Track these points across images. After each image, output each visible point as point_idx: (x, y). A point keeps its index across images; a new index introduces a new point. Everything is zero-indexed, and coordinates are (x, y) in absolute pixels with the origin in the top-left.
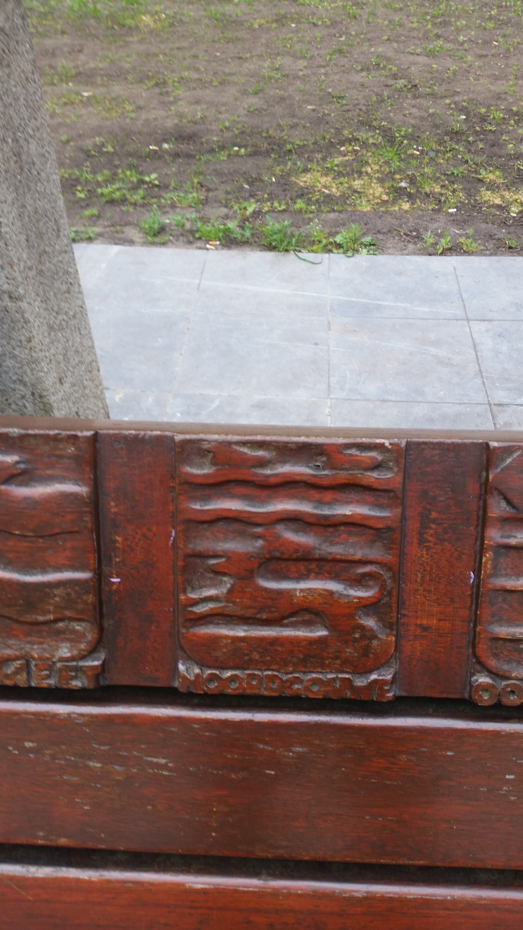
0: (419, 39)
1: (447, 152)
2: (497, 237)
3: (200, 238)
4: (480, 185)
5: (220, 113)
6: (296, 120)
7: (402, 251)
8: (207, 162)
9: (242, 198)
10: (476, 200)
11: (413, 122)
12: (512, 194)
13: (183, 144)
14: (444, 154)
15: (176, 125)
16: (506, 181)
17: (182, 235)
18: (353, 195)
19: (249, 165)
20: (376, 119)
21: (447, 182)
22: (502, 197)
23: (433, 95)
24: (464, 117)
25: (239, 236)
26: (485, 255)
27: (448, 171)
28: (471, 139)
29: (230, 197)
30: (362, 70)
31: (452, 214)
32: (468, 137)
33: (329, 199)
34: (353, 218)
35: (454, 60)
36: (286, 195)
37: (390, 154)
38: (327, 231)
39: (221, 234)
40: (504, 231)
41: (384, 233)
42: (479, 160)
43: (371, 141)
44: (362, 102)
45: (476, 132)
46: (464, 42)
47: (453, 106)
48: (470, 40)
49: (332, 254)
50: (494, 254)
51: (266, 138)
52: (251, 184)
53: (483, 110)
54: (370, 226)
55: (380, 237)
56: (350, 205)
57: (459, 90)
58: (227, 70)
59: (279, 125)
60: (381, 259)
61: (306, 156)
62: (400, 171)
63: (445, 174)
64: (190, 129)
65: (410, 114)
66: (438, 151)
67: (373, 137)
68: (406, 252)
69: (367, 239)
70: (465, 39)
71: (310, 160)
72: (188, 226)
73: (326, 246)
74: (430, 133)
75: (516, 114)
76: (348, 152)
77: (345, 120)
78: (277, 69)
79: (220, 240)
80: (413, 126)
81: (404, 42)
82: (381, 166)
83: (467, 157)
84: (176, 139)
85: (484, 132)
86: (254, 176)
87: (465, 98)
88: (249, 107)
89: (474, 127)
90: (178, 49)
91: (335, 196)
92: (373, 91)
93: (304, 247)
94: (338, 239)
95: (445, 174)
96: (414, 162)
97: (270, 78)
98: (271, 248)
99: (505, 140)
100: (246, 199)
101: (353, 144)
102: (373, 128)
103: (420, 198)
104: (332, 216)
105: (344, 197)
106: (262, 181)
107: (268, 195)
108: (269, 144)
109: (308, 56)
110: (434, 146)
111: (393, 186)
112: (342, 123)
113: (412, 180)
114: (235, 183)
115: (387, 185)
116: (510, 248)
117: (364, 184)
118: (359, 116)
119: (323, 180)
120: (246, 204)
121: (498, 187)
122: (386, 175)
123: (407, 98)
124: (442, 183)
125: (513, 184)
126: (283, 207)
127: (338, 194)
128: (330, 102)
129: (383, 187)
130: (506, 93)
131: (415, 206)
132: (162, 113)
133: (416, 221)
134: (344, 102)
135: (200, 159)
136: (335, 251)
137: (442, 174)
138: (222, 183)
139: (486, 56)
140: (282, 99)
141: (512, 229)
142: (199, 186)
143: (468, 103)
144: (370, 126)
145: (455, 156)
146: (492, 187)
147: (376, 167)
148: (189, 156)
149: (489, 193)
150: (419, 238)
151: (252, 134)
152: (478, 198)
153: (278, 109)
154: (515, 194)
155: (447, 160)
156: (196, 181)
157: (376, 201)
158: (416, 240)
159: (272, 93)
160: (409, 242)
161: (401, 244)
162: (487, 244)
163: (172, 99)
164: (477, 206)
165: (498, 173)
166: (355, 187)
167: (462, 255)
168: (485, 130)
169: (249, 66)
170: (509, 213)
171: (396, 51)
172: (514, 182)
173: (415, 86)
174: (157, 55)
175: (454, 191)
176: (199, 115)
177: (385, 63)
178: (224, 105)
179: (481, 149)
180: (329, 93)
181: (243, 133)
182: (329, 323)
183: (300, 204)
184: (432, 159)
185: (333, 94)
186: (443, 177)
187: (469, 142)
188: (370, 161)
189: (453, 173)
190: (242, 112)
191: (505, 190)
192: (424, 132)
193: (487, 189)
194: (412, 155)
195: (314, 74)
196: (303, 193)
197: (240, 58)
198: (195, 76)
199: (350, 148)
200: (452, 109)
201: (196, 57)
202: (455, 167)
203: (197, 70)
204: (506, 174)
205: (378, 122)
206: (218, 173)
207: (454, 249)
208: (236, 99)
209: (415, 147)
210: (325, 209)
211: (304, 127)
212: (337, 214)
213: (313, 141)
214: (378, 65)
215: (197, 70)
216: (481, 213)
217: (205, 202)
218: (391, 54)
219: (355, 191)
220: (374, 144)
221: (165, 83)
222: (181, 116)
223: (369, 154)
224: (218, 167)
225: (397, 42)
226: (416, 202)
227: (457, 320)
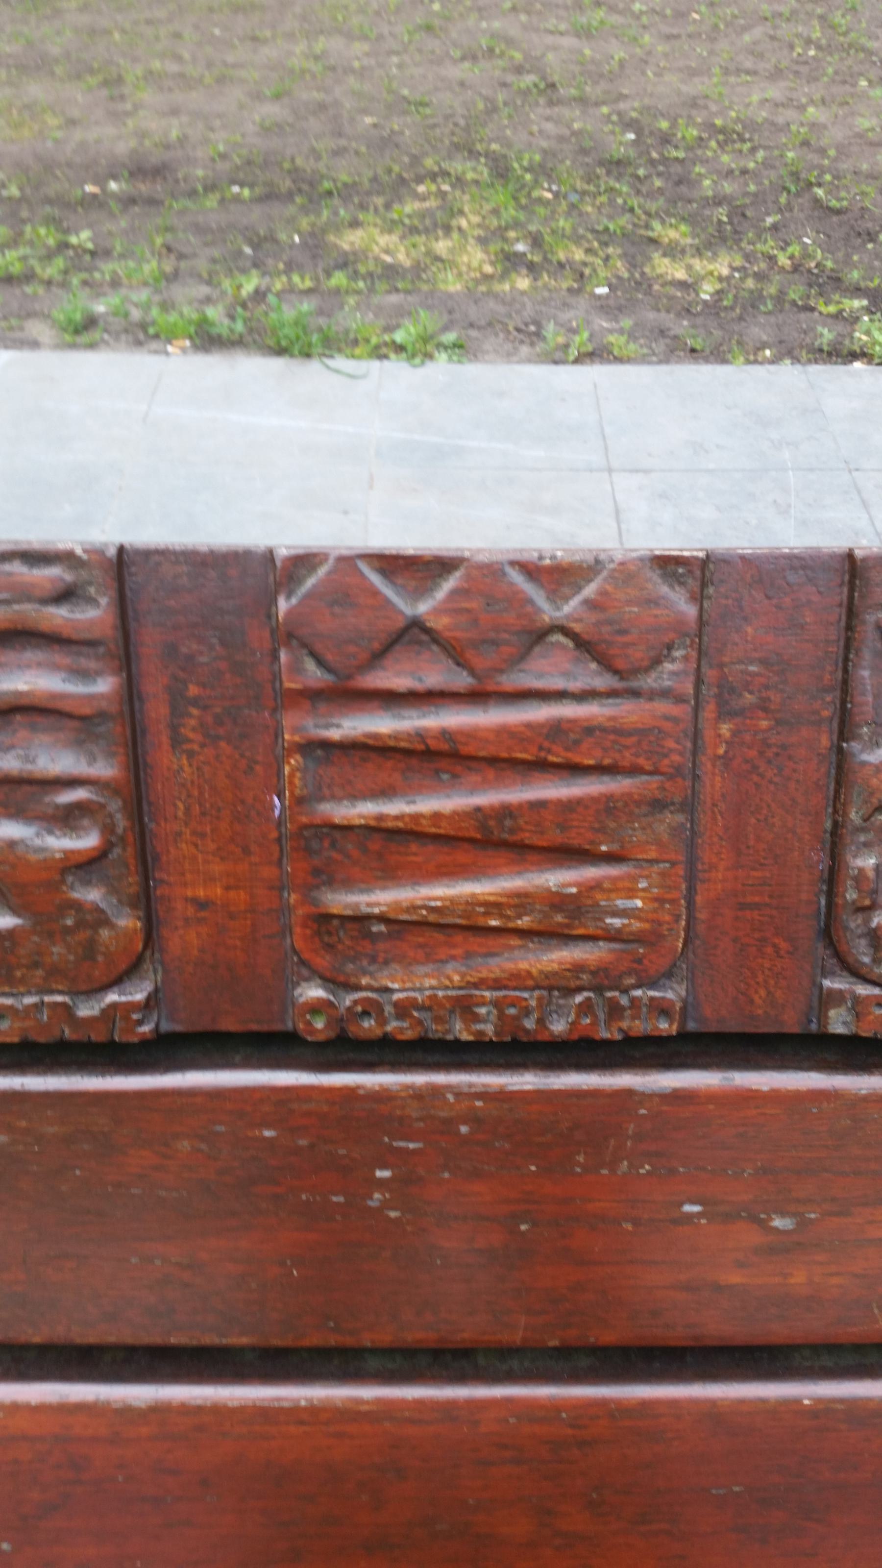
0: (566, 8)
1: (600, 194)
2: (672, 333)
3: (157, 336)
4: (652, 247)
5: (212, 129)
6: (343, 142)
7: (509, 356)
8: (182, 212)
9: (238, 269)
10: (643, 274)
11: (544, 144)
12: (705, 262)
13: (144, 182)
14: (595, 197)
15: (134, 152)
16: (697, 241)
17: (126, 331)
18: (433, 264)
19: (255, 216)
20: (481, 140)
21: (596, 244)
22: (689, 268)
23: (582, 101)
24: (631, 136)
25: (225, 332)
26: (650, 363)
27: (599, 224)
28: (641, 172)
29: (218, 267)
30: (463, 58)
31: (600, 297)
32: (637, 168)
33: (391, 272)
34: (430, 301)
35: (623, 42)
36: (316, 265)
37: (500, 196)
38: (381, 322)
39: (192, 330)
40: (685, 323)
41: (480, 328)
42: (653, 206)
43: (470, 176)
44: (460, 111)
45: (652, 162)
46: (641, 12)
47: (615, 118)
48: (653, 11)
49: (386, 363)
50: (665, 361)
51: (289, 172)
52: (255, 247)
53: (664, 125)
54: (457, 316)
55: (473, 333)
56: (428, 281)
57: (625, 91)
58: (230, 59)
59: (313, 150)
60: (471, 370)
61: (356, 200)
62: (516, 224)
63: (594, 231)
64: (156, 158)
65: (541, 132)
66: (584, 193)
67: (474, 170)
68: (515, 358)
69: (450, 337)
70: (644, 8)
71: (363, 207)
72: (136, 314)
73: (377, 347)
74: (573, 162)
75: (722, 131)
76: (429, 193)
77: (428, 142)
78: (317, 58)
79: (191, 338)
80: (544, 152)
81: (540, 13)
82: (484, 217)
83: (634, 202)
84: (132, 174)
85: (665, 160)
86: (262, 233)
87: (636, 104)
88: (263, 120)
89: (649, 153)
90: (149, 22)
91: (402, 266)
92: (480, 94)
93: (340, 350)
94: (399, 337)
95: (594, 231)
96: (541, 211)
97: (303, 72)
98: (281, 351)
99: (700, 174)
100: (244, 271)
101: (439, 180)
102: (473, 154)
103: (548, 272)
104: (394, 299)
105: (418, 269)
106: (275, 241)
107: (285, 264)
108: (294, 182)
109: (373, 36)
110: (579, 185)
111: (502, 250)
112: (422, 146)
113: (536, 241)
114: (229, 244)
115: (492, 248)
116: (693, 350)
117: (454, 247)
118: (453, 134)
119: (384, 240)
120: (242, 279)
121: (683, 252)
122: (494, 233)
123: (537, 104)
124: (586, 245)
125: (709, 245)
126: (308, 284)
127: (408, 263)
128: (405, 113)
129: (487, 252)
130: (706, 97)
131: (540, 283)
132: (110, 131)
133: (537, 308)
134: (428, 111)
135: (171, 207)
136: (392, 356)
137: (587, 229)
138: (206, 244)
139: (677, 37)
140: (322, 107)
141: (699, 321)
142: (164, 251)
143: (641, 113)
144: (470, 152)
145: (612, 202)
146: (673, 251)
147: (476, 219)
148: (153, 202)
149: (666, 261)
150: (538, 335)
151: (266, 164)
152: (647, 270)
153: (314, 124)
154: (710, 263)
155: (599, 208)
156: (159, 241)
157: (472, 275)
158: (535, 339)
159: (305, 96)
160: (522, 342)
161: (508, 346)
162: (654, 345)
163: (128, 106)
164: (644, 284)
165: (683, 228)
166: (438, 252)
167: (609, 362)
168: (667, 159)
169: (268, 52)
170: (697, 294)
171: (525, 28)
172: (710, 244)
173: (553, 86)
174: (108, 32)
175: (607, 259)
176: (174, 134)
177: (503, 46)
178: (220, 116)
179: (659, 188)
180: (404, 98)
181: (249, 163)
182: (371, 478)
183: (339, 279)
184: (573, 206)
185: (411, 99)
186: (590, 236)
187: (638, 178)
188: (466, 209)
189: (607, 229)
190: (250, 128)
191: (693, 256)
192: (562, 162)
193: (665, 255)
194: (540, 201)
195: (381, 65)
196: (346, 262)
197: (254, 39)
198: (173, 67)
199: (433, 188)
200: (613, 123)
201: (177, 36)
202: (611, 218)
203: (179, 58)
204: (698, 230)
205: (484, 145)
206: (199, 229)
207: (597, 354)
208: (241, 107)
209: (546, 185)
210: (381, 286)
211: (357, 153)
212: (402, 296)
213: (370, 174)
214: (491, 50)
215: (179, 58)
216: (650, 294)
217: (174, 277)
218: (514, 32)
219: (438, 259)
220: (476, 182)
221: (120, 80)
222: (142, 135)
223: (467, 197)
224: (201, 219)
225: (528, 13)
226: (542, 277)
227: (591, 471)
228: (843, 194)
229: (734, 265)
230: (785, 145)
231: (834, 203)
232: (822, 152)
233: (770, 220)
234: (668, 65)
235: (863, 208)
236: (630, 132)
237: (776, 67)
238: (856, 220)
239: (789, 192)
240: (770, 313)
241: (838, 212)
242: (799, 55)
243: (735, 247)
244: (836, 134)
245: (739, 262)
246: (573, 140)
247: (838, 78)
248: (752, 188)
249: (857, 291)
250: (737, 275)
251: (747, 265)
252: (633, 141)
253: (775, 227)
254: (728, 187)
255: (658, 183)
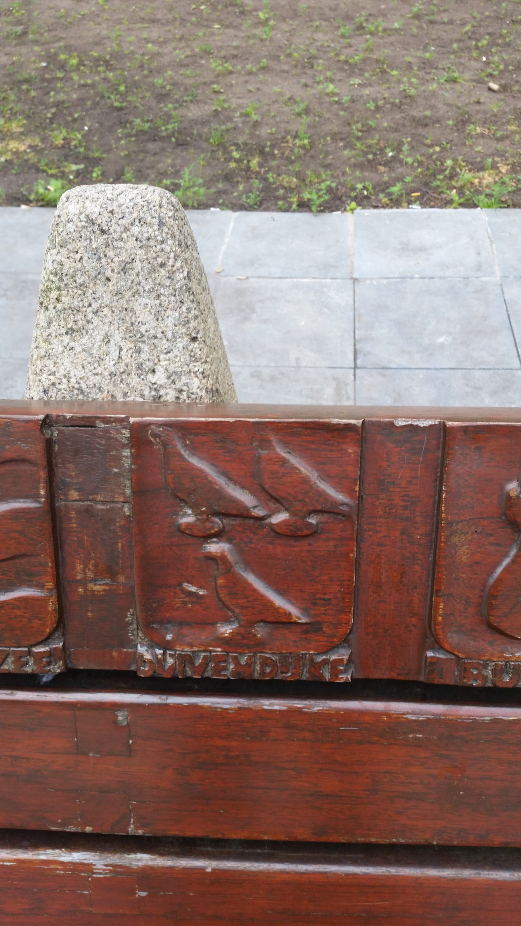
24: (44, 64)
45: (43, 80)
123: (10, 45)
130: (109, 38)
168: (54, 78)
179: (33, 97)
228: (129, 98)
229: (33, 144)
230: (130, 67)
231: (117, 104)
232: (143, 70)
233: (76, 115)
234: (109, 18)
235: (135, 107)
236: (44, 61)
237: (174, 17)
238: (125, 114)
239: (103, 97)
240: (17, 174)
241: (120, 109)
242: (194, 9)
243: (42, 133)
244: (167, 59)
245: (37, 141)
246: (8, 67)
247: (205, 23)
248: (75, 96)
249: (86, 159)
250: (28, 150)
251: (40, 144)
252: (45, 67)
253: (75, 120)
254: (62, 96)
255: (33, 93)
